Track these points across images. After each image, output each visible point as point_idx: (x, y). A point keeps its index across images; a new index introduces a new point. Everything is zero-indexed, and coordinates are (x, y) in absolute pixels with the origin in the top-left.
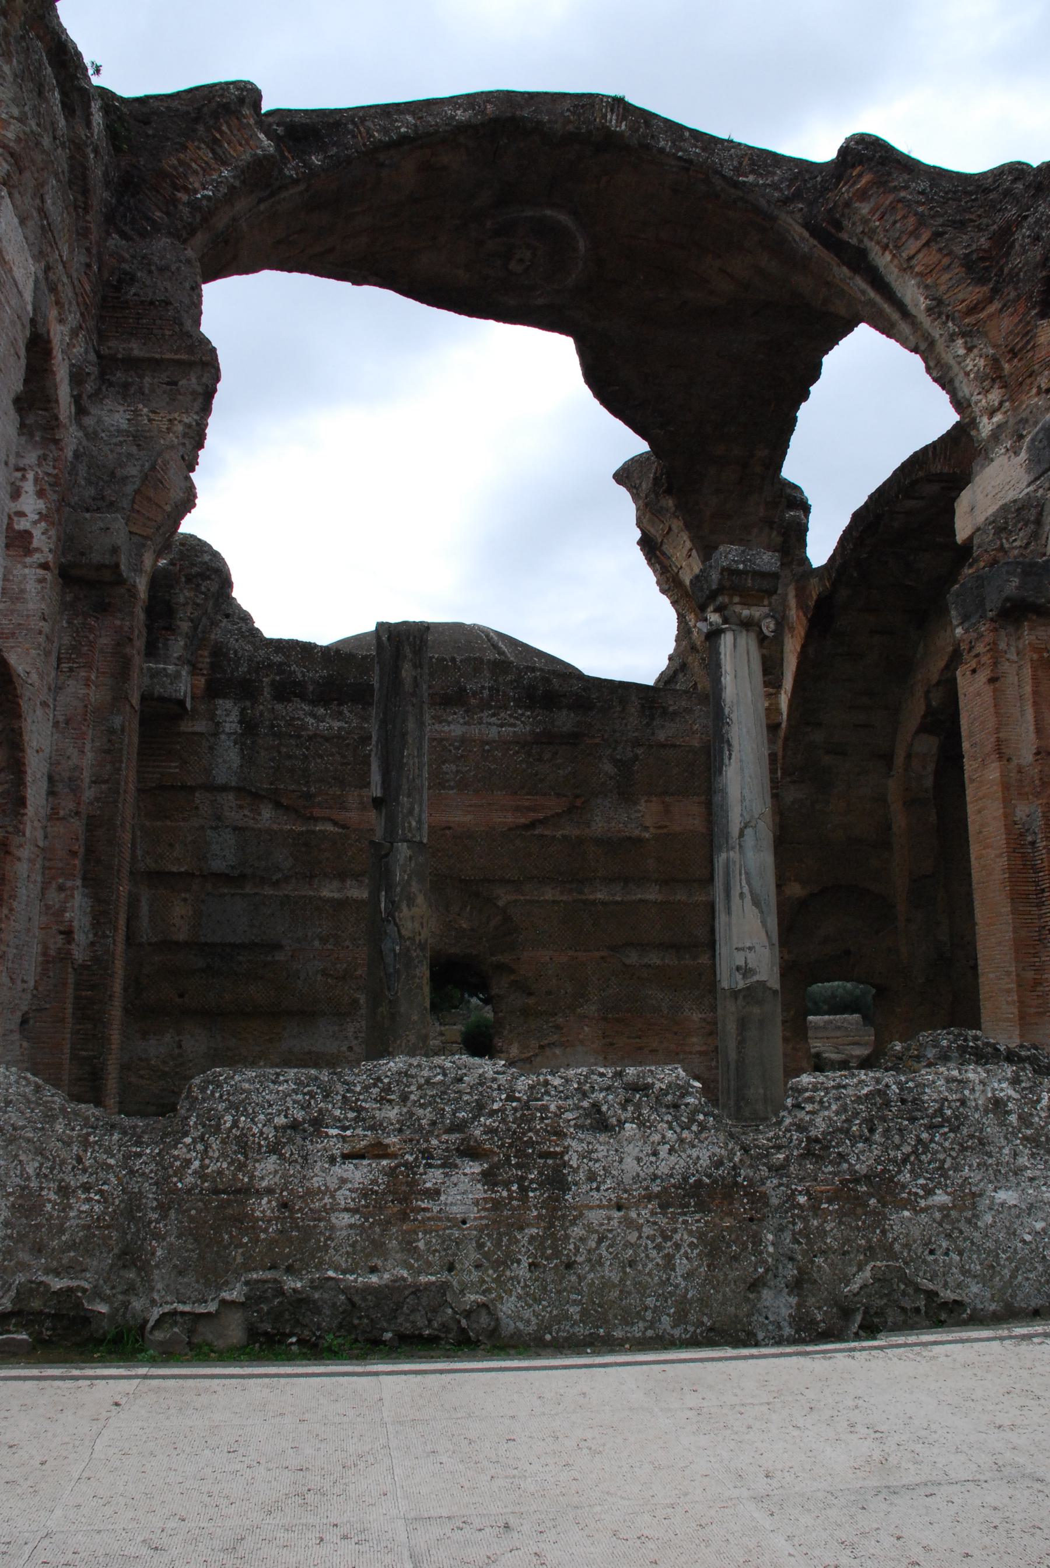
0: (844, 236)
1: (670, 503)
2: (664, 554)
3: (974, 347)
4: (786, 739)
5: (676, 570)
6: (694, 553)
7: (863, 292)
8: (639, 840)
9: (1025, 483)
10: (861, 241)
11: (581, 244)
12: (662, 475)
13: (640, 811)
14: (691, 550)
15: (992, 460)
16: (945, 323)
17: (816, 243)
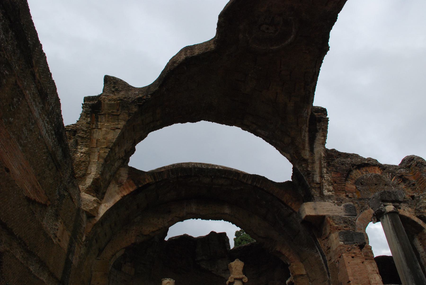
0: (318, 124)
1: (135, 109)
2: (97, 118)
3: (328, 173)
4: (95, 225)
5: (94, 126)
6: (119, 131)
7: (304, 136)
8: (53, 243)
9: (343, 214)
10: (320, 129)
11: (275, 48)
12: (144, 99)
13: (56, 226)
14: (119, 129)
15: (325, 201)
16: (325, 163)
17: (309, 117)
